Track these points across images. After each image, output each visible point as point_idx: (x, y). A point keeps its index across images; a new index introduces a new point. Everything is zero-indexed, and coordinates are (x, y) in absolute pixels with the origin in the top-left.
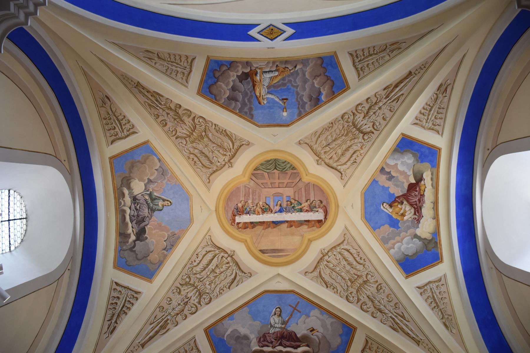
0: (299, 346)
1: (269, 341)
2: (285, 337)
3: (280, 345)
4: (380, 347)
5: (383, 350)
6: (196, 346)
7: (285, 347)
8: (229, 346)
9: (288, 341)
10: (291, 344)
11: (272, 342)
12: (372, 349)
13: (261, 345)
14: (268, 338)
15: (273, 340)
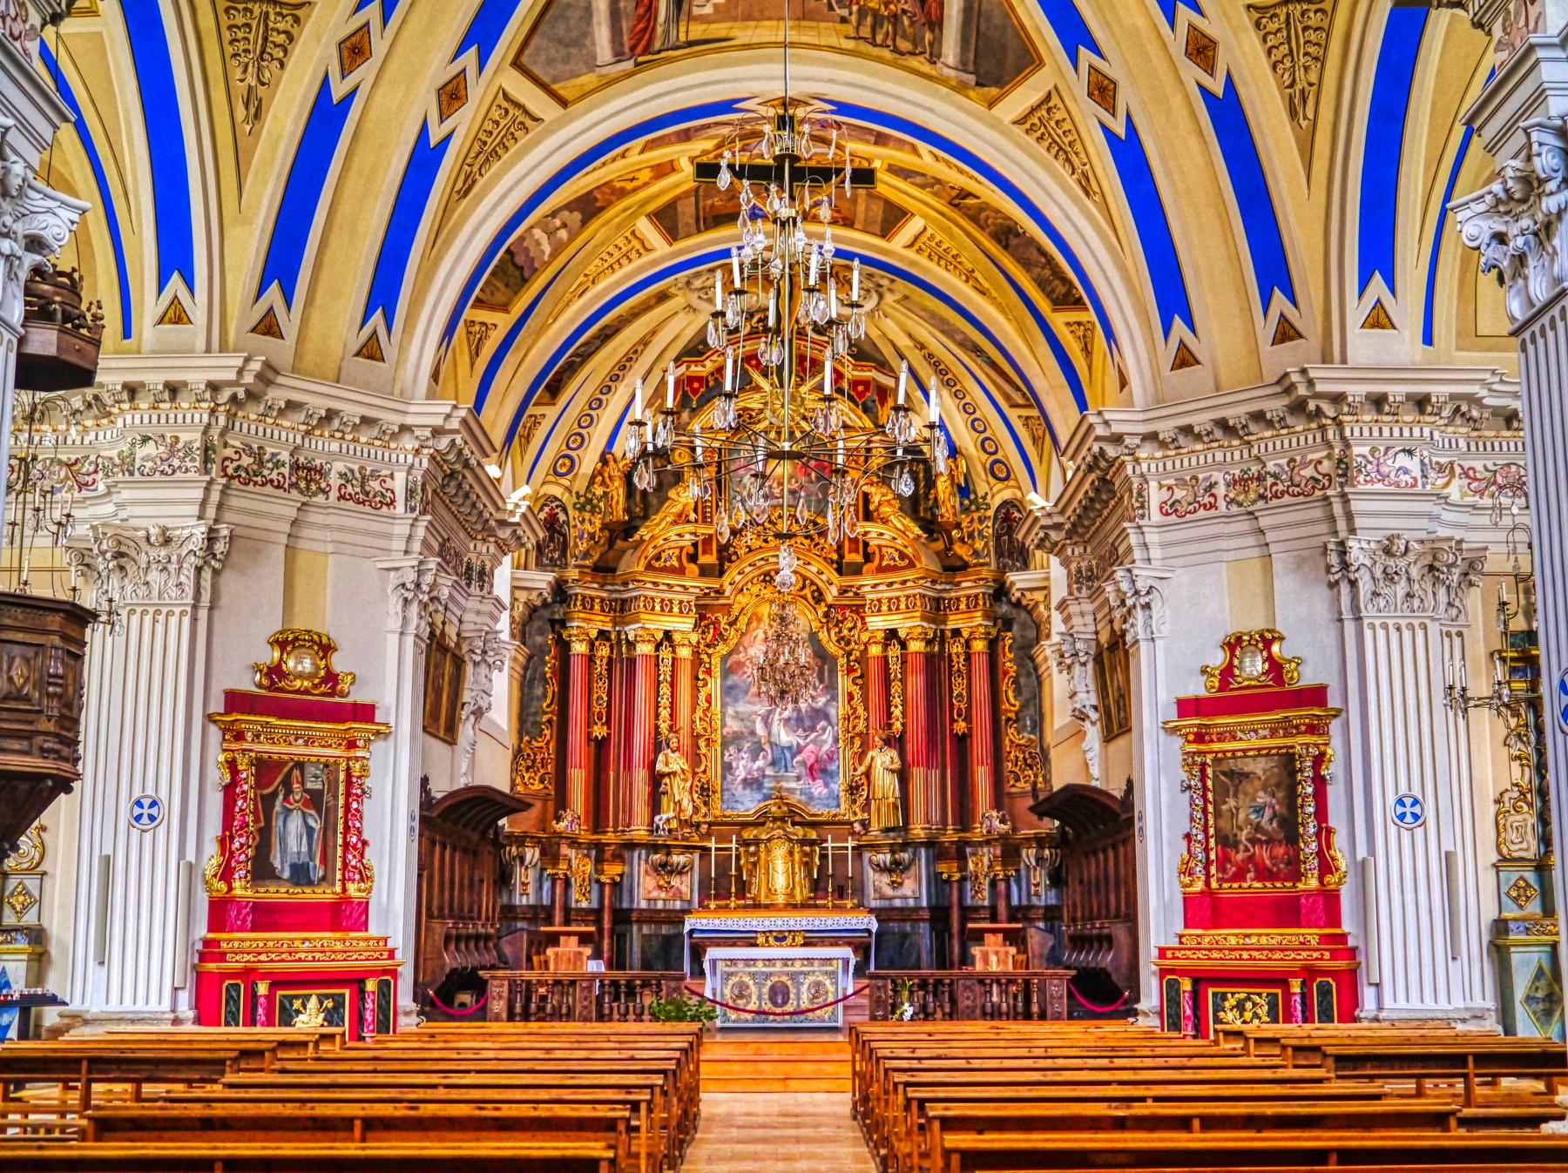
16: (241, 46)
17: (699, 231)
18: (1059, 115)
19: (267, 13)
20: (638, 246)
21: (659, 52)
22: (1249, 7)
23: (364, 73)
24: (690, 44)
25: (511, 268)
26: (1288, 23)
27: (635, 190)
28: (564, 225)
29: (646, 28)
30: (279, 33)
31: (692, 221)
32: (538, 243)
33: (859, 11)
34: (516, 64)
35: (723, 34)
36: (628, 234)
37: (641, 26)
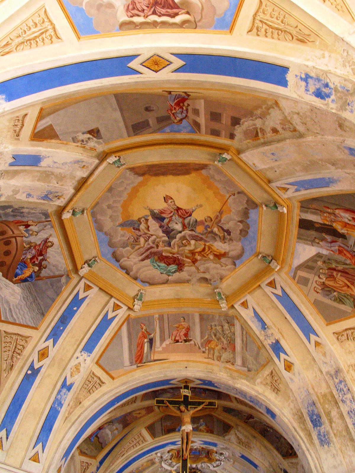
0: (177, 14)
1: (140, 9)
2: (159, 3)
3: (154, 13)
4: (276, 8)
5: (280, 13)
6: (48, 18)
7: (160, 16)
8: (90, 17)
9: (163, 7)
10: (167, 12)
11: (143, 10)
12: (266, 13)
13: (130, 14)
14: (138, 6)
15: (145, 8)
16: (8, 348)
17: (163, 435)
18: (276, 378)
19: (17, 339)
20: (142, 439)
21: (145, 363)
22: (334, 333)
23: (46, 362)
24: (155, 361)
25: (98, 442)
26: (348, 337)
27: (141, 417)
28: (117, 429)
29: (141, 354)
30: (20, 346)
31: (160, 431)
32: (108, 435)
33: (209, 348)
34: (97, 363)
35: (165, 358)
36: (139, 434)
37: (139, 354)
